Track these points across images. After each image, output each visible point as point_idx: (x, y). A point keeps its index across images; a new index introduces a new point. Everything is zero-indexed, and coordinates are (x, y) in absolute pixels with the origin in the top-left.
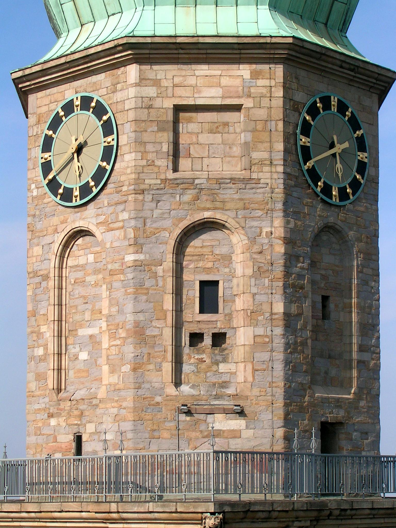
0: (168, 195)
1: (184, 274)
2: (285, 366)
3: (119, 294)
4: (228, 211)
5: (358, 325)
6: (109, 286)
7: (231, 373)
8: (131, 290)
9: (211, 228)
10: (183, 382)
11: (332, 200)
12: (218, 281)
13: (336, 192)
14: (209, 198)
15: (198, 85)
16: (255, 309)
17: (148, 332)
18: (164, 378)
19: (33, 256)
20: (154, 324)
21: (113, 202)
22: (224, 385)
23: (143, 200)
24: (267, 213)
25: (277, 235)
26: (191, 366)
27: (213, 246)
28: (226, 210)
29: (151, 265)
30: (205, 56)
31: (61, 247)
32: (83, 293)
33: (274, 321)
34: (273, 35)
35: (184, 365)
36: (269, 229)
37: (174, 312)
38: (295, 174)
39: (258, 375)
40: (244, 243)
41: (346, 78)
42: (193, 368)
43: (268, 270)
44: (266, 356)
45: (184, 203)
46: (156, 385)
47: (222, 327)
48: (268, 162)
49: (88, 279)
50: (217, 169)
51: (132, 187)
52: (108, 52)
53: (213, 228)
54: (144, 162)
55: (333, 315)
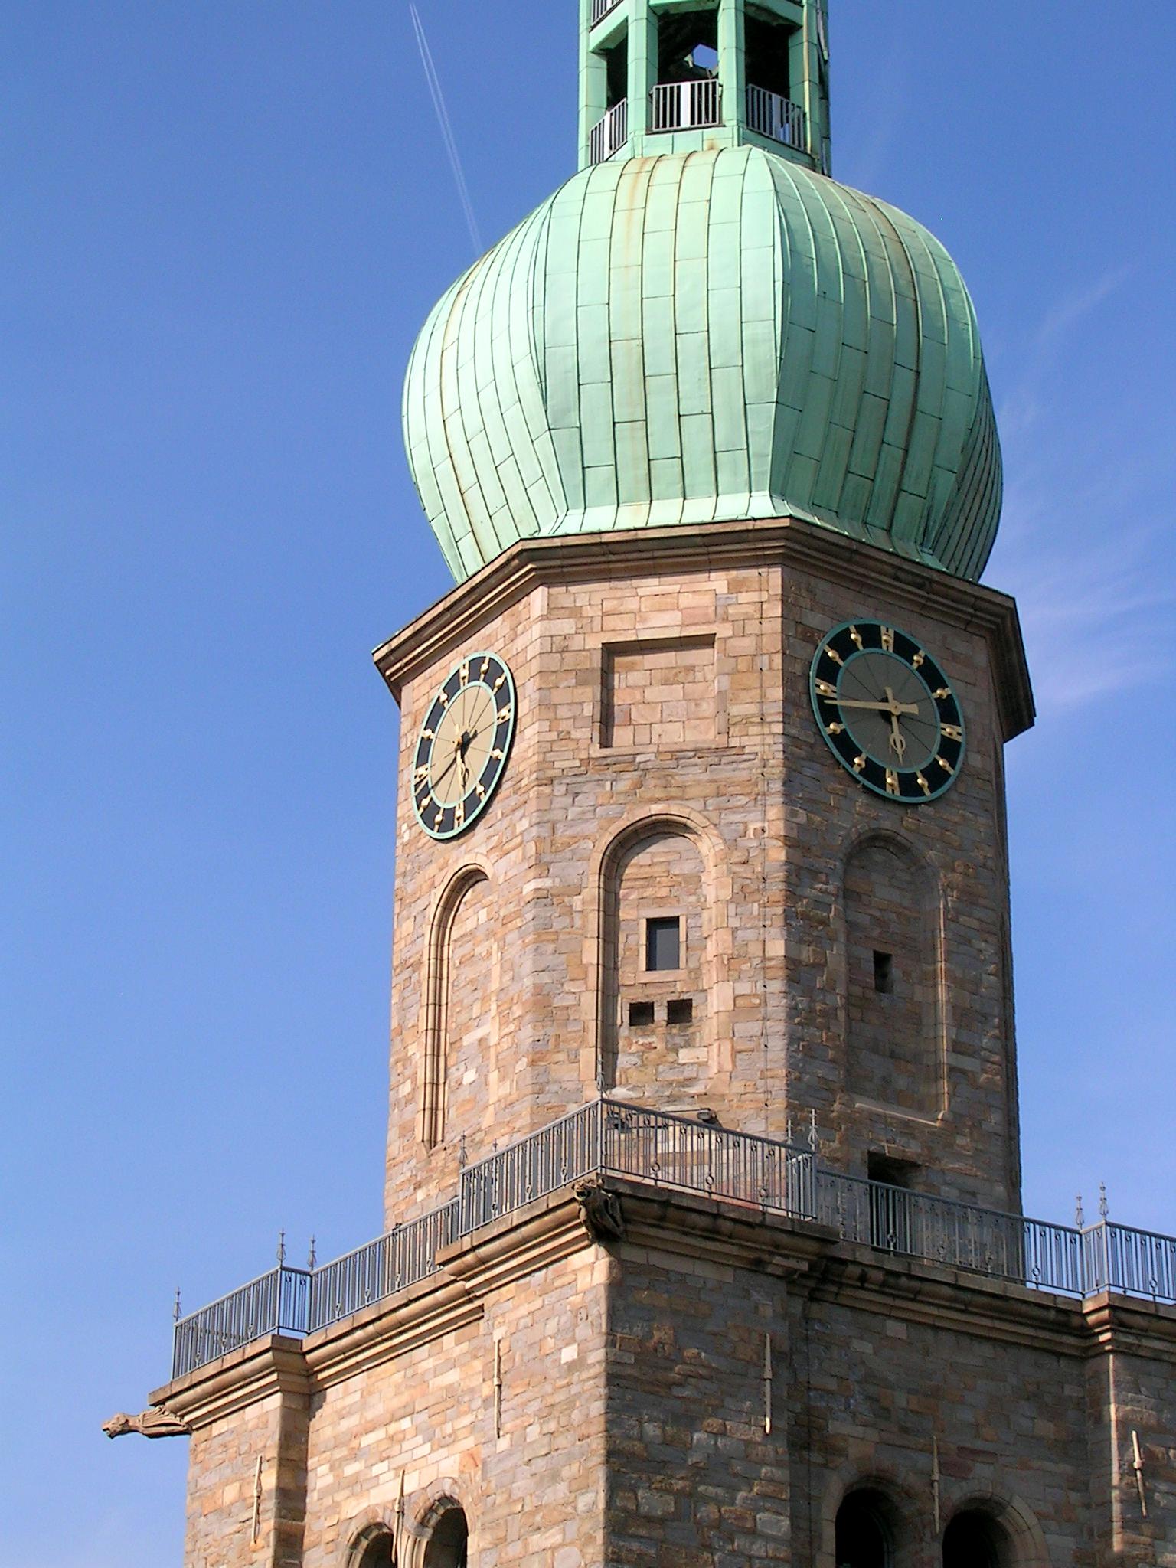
0: (590, 785)
1: (620, 911)
2: (789, 1044)
3: (512, 952)
4: (691, 801)
5: (950, 1007)
6: (501, 943)
7: (700, 1064)
8: (530, 938)
9: (665, 833)
10: (617, 1082)
11: (885, 790)
12: (678, 918)
13: (893, 779)
14: (658, 782)
15: (643, 609)
16: (736, 953)
17: (557, 1002)
18: (581, 1074)
19: (401, 939)
20: (566, 988)
21: (507, 811)
22: (689, 1082)
23: (551, 794)
24: (756, 799)
25: (772, 833)
26: (631, 1057)
27: (669, 862)
28: (687, 799)
29: (563, 895)
30: (650, 562)
31: (439, 908)
32: (471, 976)
33: (768, 971)
34: (756, 517)
35: (620, 1056)
36: (759, 825)
37: (600, 967)
38: (808, 740)
39: (740, 1059)
40: (717, 849)
41: (910, 601)
42: (634, 1059)
43: (758, 890)
44: (755, 1028)
45: (617, 794)
46: (570, 1086)
47: (684, 990)
48: (759, 720)
49: (478, 950)
50: (676, 740)
51: (534, 776)
52: (500, 575)
53: (670, 833)
54: (554, 736)
55: (898, 988)
